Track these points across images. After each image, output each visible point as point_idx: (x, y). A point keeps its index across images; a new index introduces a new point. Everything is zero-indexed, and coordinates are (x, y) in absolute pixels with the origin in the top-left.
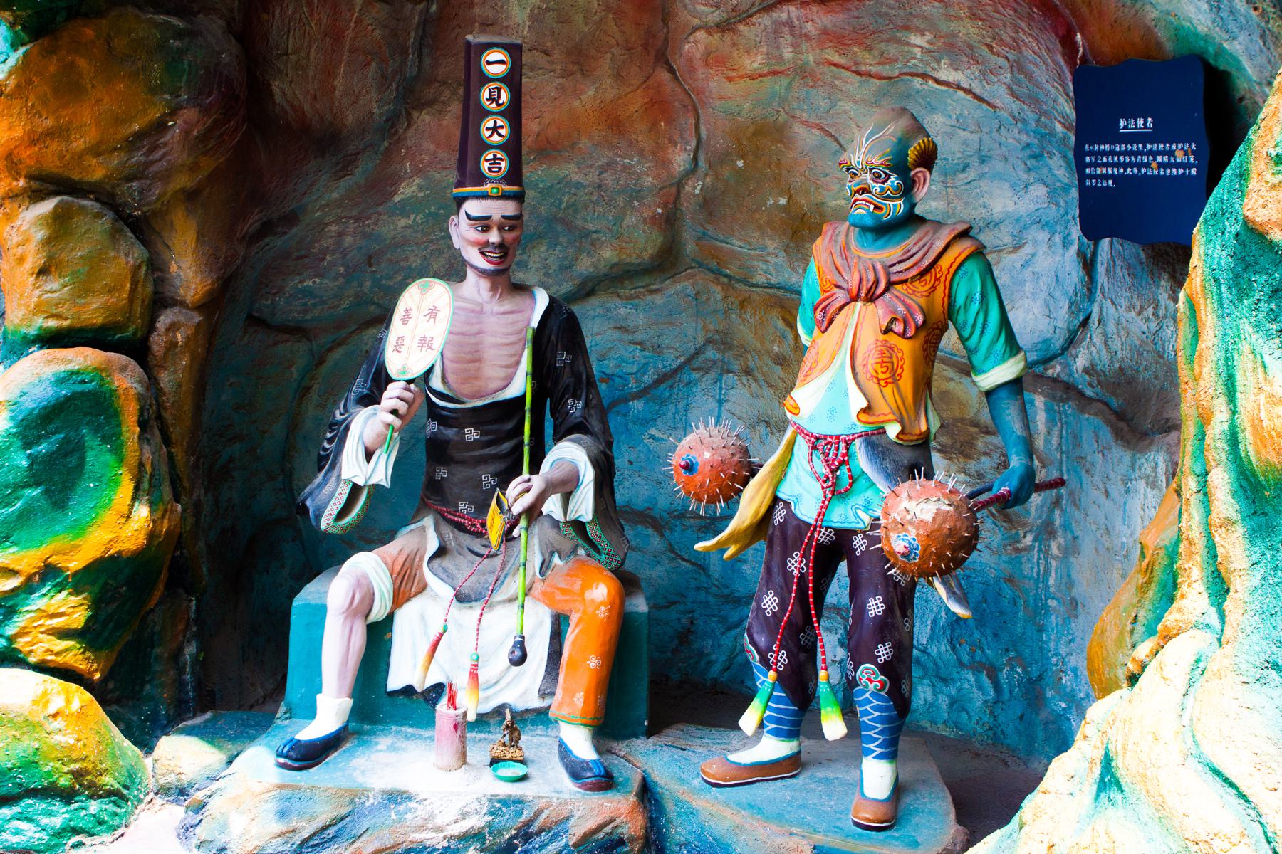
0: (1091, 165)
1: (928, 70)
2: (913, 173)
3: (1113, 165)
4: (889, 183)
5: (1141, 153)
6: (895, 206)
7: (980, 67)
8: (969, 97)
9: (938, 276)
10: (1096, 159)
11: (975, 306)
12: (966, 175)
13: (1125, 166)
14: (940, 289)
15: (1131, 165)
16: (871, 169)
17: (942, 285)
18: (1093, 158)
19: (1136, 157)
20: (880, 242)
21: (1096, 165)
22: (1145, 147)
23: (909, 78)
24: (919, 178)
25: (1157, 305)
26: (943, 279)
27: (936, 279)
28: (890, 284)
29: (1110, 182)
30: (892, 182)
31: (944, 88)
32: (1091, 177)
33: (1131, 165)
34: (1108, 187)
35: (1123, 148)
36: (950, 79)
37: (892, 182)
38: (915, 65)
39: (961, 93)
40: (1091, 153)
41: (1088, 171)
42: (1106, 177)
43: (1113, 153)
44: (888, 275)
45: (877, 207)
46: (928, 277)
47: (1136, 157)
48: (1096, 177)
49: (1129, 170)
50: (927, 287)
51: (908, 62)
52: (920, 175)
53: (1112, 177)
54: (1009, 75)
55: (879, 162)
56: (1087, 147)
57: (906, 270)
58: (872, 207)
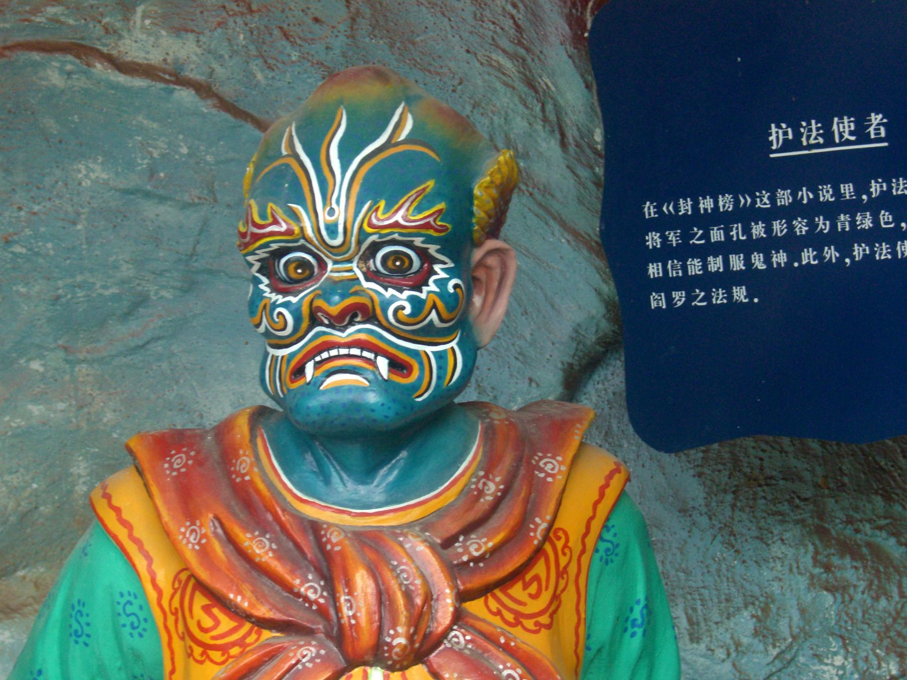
0: (664, 254)
1: (94, 34)
2: (478, 254)
3: (747, 248)
4: (432, 287)
5: (853, 207)
6: (440, 356)
7: (255, 21)
8: (206, 107)
9: (563, 561)
10: (686, 236)
11: (633, 644)
12: (134, 325)
13: (793, 244)
14: (569, 599)
15: (816, 240)
16: (375, 248)
17: (572, 587)
18: (673, 238)
19: (832, 219)
20: (388, 475)
21: (684, 252)
22: (862, 187)
23: (36, 56)
24: (488, 268)
25: (765, 610)
26: (573, 569)
27: (560, 574)
28: (462, 597)
29: (740, 294)
30: (441, 283)
31: (139, 83)
32: (666, 285)
33: (816, 240)
34: (732, 304)
35: (784, 197)
36: (155, 57)
37: (441, 283)
38: (54, 20)
39: (185, 95)
40: (662, 224)
41: (654, 270)
42: (728, 279)
43: (747, 216)
44: (454, 570)
45: (396, 365)
46: (540, 568)
47: (832, 219)
48: (687, 283)
49: (808, 256)
50: (546, 597)
51: (36, 11)
52: (492, 261)
53: (748, 277)
54: (339, 42)
55: (419, 218)
56: (649, 210)
57: (494, 551)
58: (383, 363)
